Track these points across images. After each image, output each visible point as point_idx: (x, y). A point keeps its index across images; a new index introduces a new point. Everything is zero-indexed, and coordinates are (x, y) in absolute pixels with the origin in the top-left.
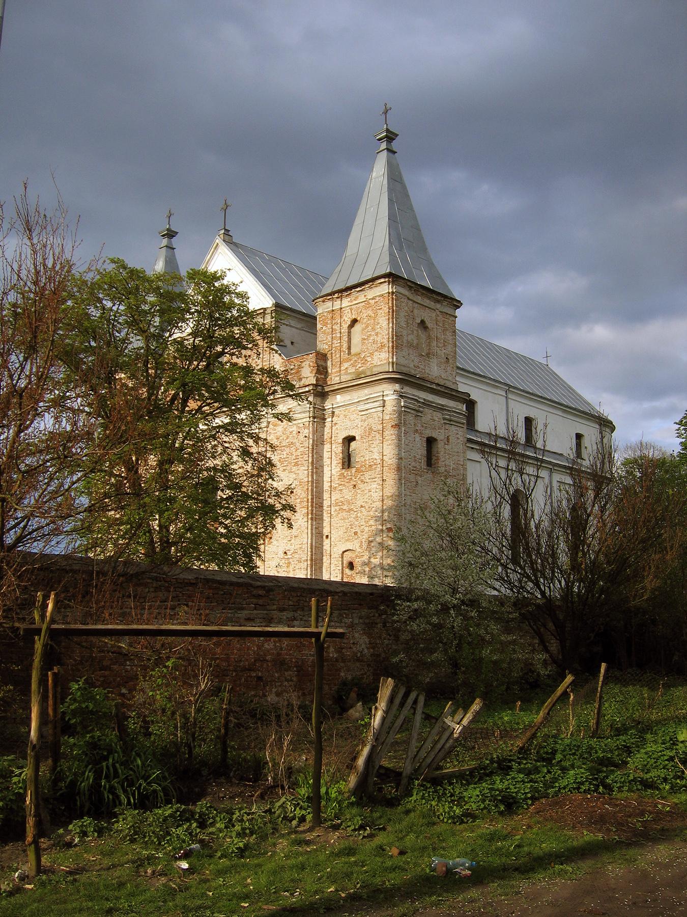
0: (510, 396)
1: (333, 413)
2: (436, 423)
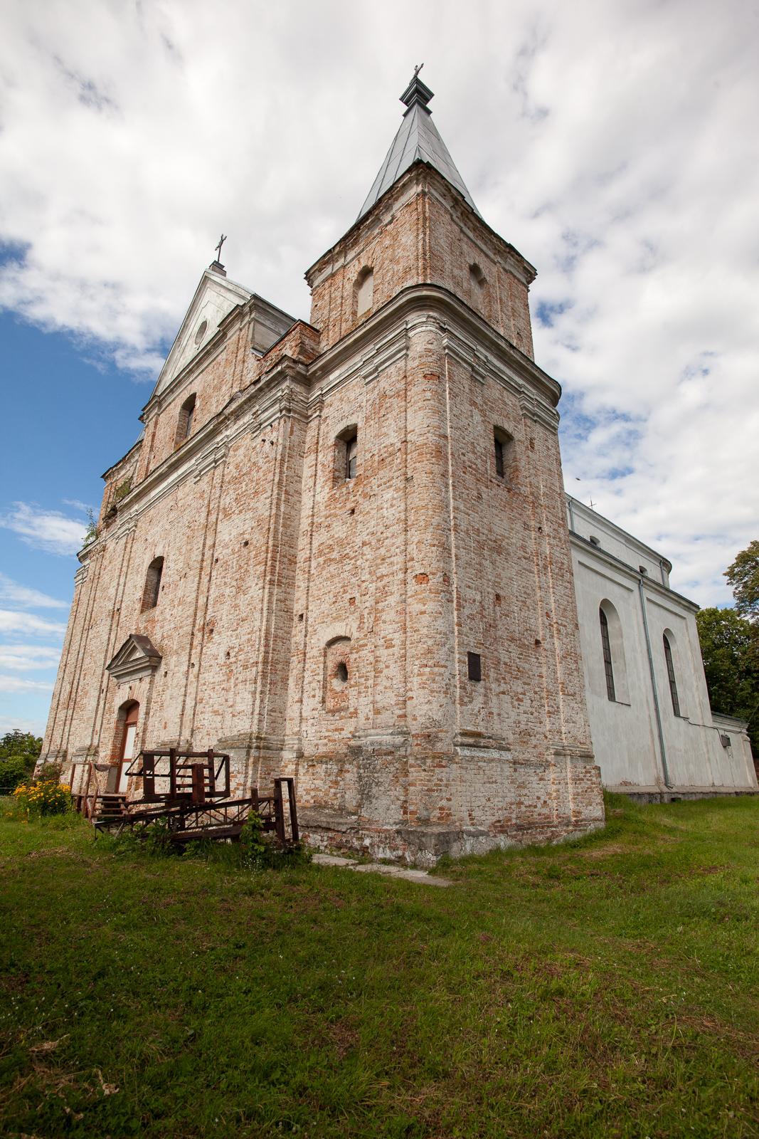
0: (573, 510)
1: (322, 402)
2: (510, 409)
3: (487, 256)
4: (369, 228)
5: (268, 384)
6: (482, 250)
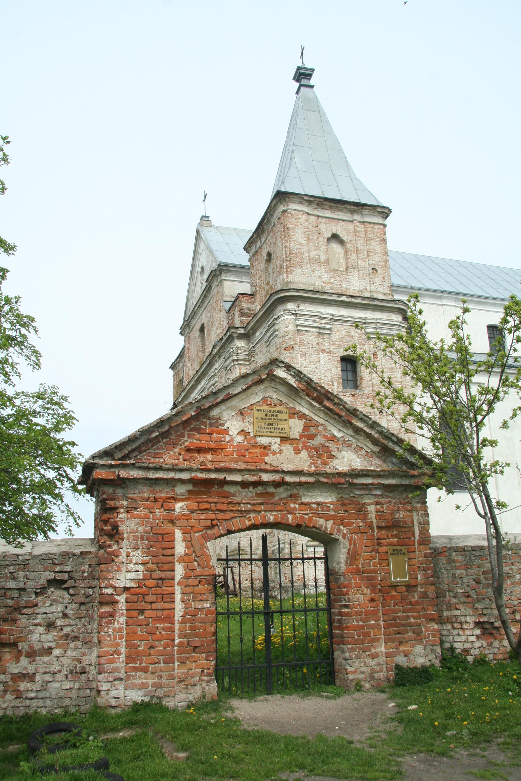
1: (254, 351)
3: (344, 221)
4: (266, 224)
5: (227, 340)
6: (339, 220)
